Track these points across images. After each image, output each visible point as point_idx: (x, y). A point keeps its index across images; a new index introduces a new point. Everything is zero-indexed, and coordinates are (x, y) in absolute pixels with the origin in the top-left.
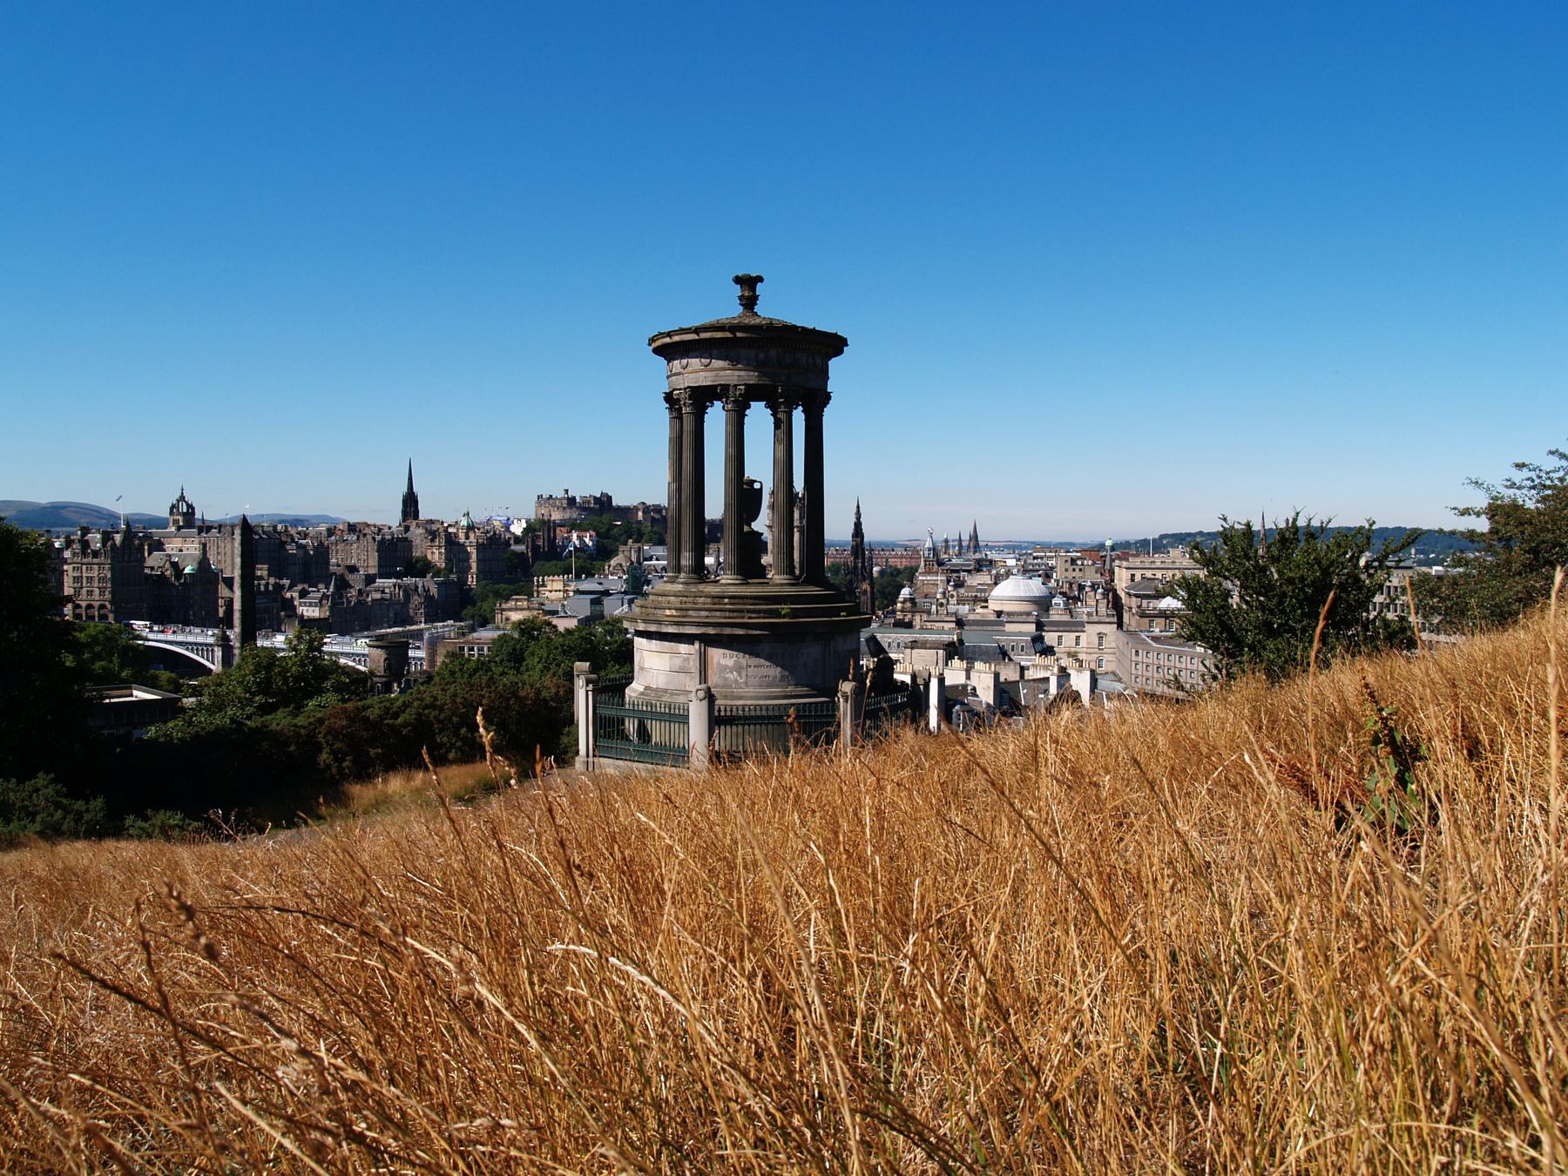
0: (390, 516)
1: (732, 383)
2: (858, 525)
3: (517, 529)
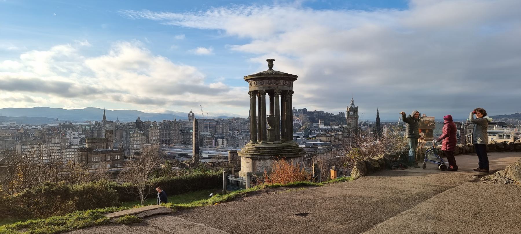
2: (378, 116)
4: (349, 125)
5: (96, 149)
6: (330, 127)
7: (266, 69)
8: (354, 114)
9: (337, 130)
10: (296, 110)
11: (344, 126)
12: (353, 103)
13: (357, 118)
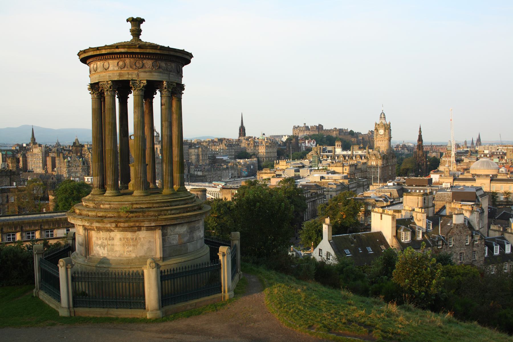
0: (234, 135)
1: (106, 80)
2: (420, 137)
3: (284, 139)
7: (128, 37)
8: (384, 134)
9: (361, 156)
10: (308, 127)
11: (370, 151)
13: (390, 138)
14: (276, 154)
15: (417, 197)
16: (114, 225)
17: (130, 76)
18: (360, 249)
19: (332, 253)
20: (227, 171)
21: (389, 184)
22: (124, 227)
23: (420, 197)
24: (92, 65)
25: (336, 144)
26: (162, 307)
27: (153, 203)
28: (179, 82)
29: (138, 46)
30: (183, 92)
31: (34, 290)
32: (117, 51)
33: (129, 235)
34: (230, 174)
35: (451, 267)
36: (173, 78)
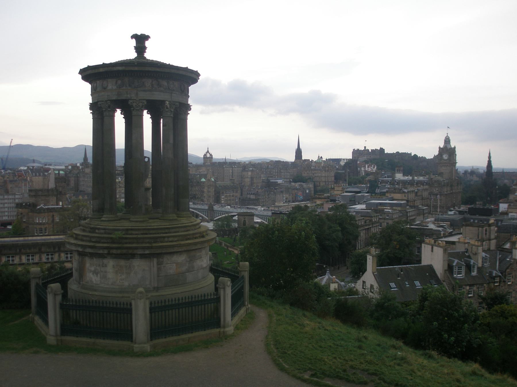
0: (291, 158)
2: (489, 162)
3: (342, 163)
4: (441, 174)
5: (42, 206)
6: (410, 178)
7: (132, 55)
8: (449, 159)
10: (368, 150)
12: (447, 141)
14: (333, 179)
15: (477, 228)
16: (106, 252)
17: (128, 96)
18: (407, 283)
19: (376, 285)
20: (281, 195)
21: (450, 213)
22: (117, 254)
23: (480, 229)
24: (93, 84)
25: (396, 169)
26: (151, 340)
27: (149, 229)
28: (183, 102)
29: (136, 63)
30: (189, 112)
31: (31, 315)
32: (115, 69)
33: (122, 262)
34: (284, 198)
35: (506, 307)
36: (177, 98)
